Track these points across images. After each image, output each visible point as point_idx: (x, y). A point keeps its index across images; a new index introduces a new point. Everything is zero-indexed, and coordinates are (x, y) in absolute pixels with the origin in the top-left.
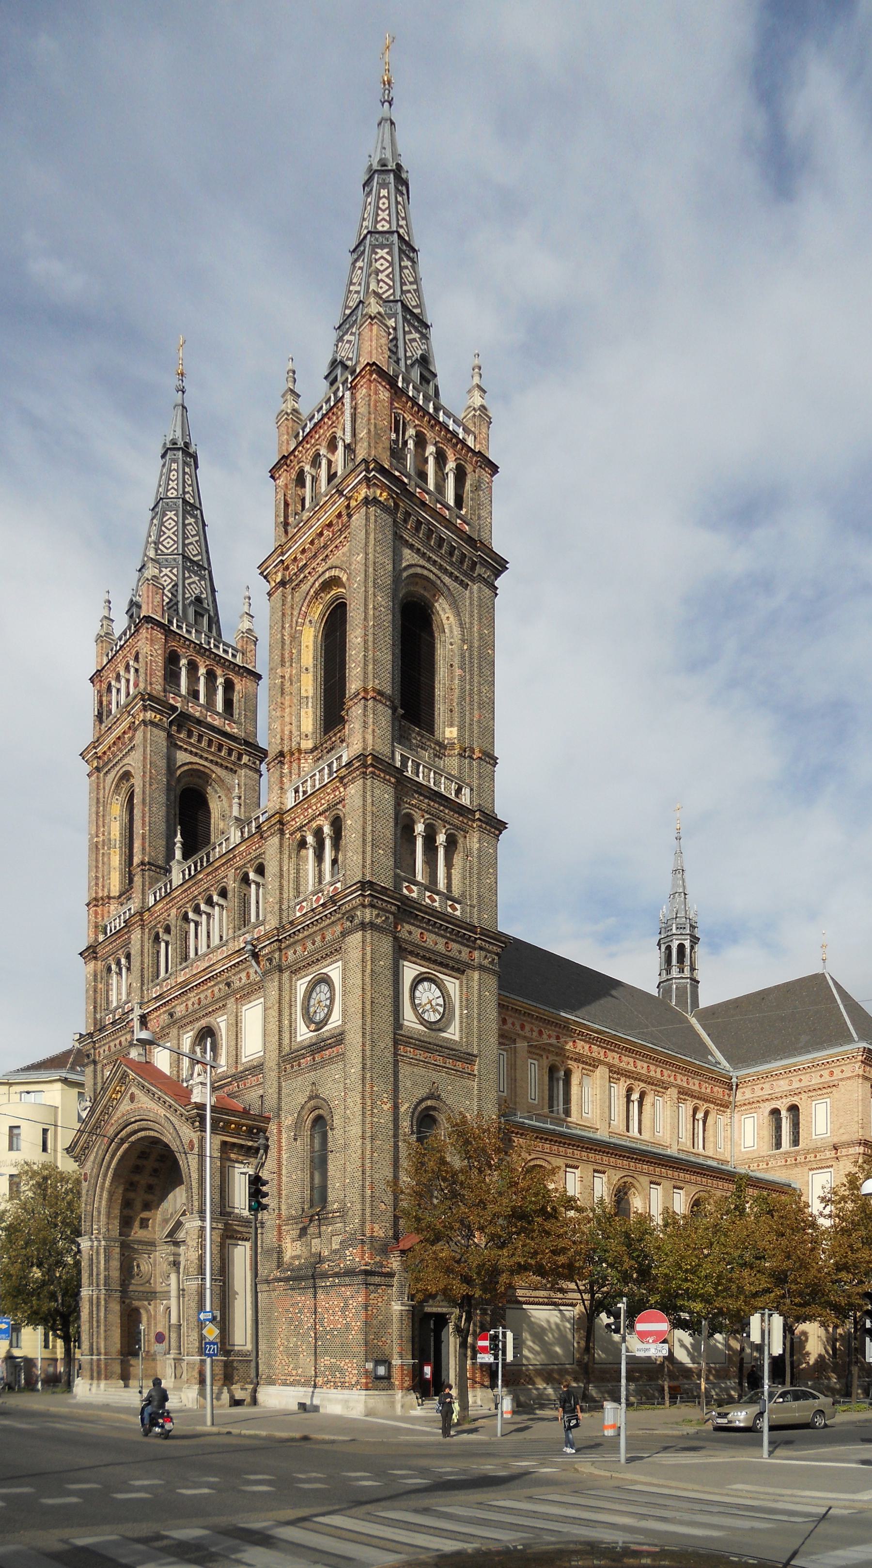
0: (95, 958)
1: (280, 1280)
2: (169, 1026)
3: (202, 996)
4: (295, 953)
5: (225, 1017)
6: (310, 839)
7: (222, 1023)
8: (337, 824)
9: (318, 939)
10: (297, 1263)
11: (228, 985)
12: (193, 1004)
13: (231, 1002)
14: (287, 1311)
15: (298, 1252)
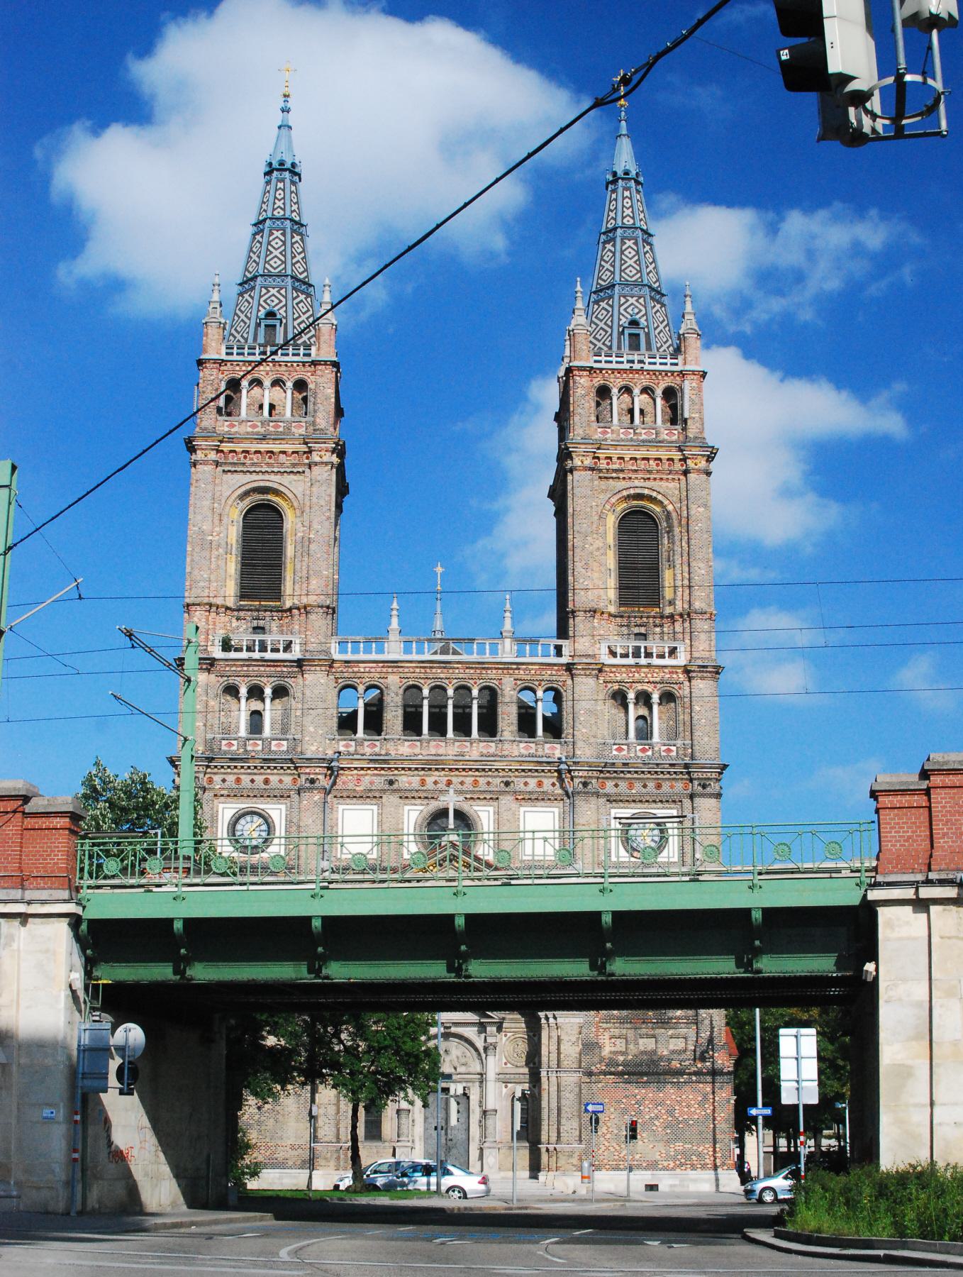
0: (209, 671)
1: (611, 1073)
2: (384, 791)
3: (454, 780)
4: (616, 786)
5: (491, 809)
6: (631, 696)
7: (484, 815)
8: (668, 697)
9: (651, 785)
10: (621, 1058)
11: (507, 784)
12: (436, 783)
13: (507, 800)
14: (619, 1102)
15: (618, 1048)
